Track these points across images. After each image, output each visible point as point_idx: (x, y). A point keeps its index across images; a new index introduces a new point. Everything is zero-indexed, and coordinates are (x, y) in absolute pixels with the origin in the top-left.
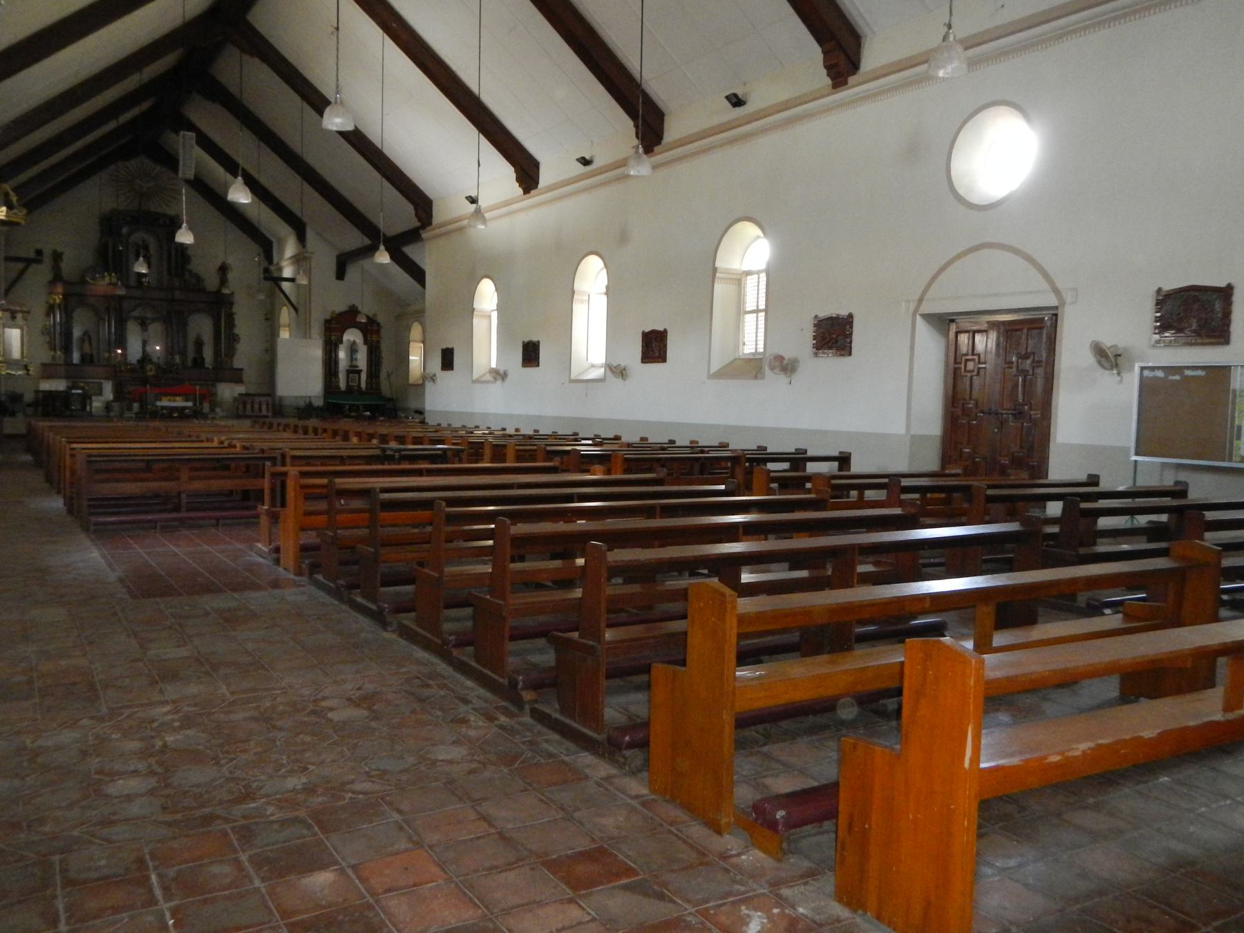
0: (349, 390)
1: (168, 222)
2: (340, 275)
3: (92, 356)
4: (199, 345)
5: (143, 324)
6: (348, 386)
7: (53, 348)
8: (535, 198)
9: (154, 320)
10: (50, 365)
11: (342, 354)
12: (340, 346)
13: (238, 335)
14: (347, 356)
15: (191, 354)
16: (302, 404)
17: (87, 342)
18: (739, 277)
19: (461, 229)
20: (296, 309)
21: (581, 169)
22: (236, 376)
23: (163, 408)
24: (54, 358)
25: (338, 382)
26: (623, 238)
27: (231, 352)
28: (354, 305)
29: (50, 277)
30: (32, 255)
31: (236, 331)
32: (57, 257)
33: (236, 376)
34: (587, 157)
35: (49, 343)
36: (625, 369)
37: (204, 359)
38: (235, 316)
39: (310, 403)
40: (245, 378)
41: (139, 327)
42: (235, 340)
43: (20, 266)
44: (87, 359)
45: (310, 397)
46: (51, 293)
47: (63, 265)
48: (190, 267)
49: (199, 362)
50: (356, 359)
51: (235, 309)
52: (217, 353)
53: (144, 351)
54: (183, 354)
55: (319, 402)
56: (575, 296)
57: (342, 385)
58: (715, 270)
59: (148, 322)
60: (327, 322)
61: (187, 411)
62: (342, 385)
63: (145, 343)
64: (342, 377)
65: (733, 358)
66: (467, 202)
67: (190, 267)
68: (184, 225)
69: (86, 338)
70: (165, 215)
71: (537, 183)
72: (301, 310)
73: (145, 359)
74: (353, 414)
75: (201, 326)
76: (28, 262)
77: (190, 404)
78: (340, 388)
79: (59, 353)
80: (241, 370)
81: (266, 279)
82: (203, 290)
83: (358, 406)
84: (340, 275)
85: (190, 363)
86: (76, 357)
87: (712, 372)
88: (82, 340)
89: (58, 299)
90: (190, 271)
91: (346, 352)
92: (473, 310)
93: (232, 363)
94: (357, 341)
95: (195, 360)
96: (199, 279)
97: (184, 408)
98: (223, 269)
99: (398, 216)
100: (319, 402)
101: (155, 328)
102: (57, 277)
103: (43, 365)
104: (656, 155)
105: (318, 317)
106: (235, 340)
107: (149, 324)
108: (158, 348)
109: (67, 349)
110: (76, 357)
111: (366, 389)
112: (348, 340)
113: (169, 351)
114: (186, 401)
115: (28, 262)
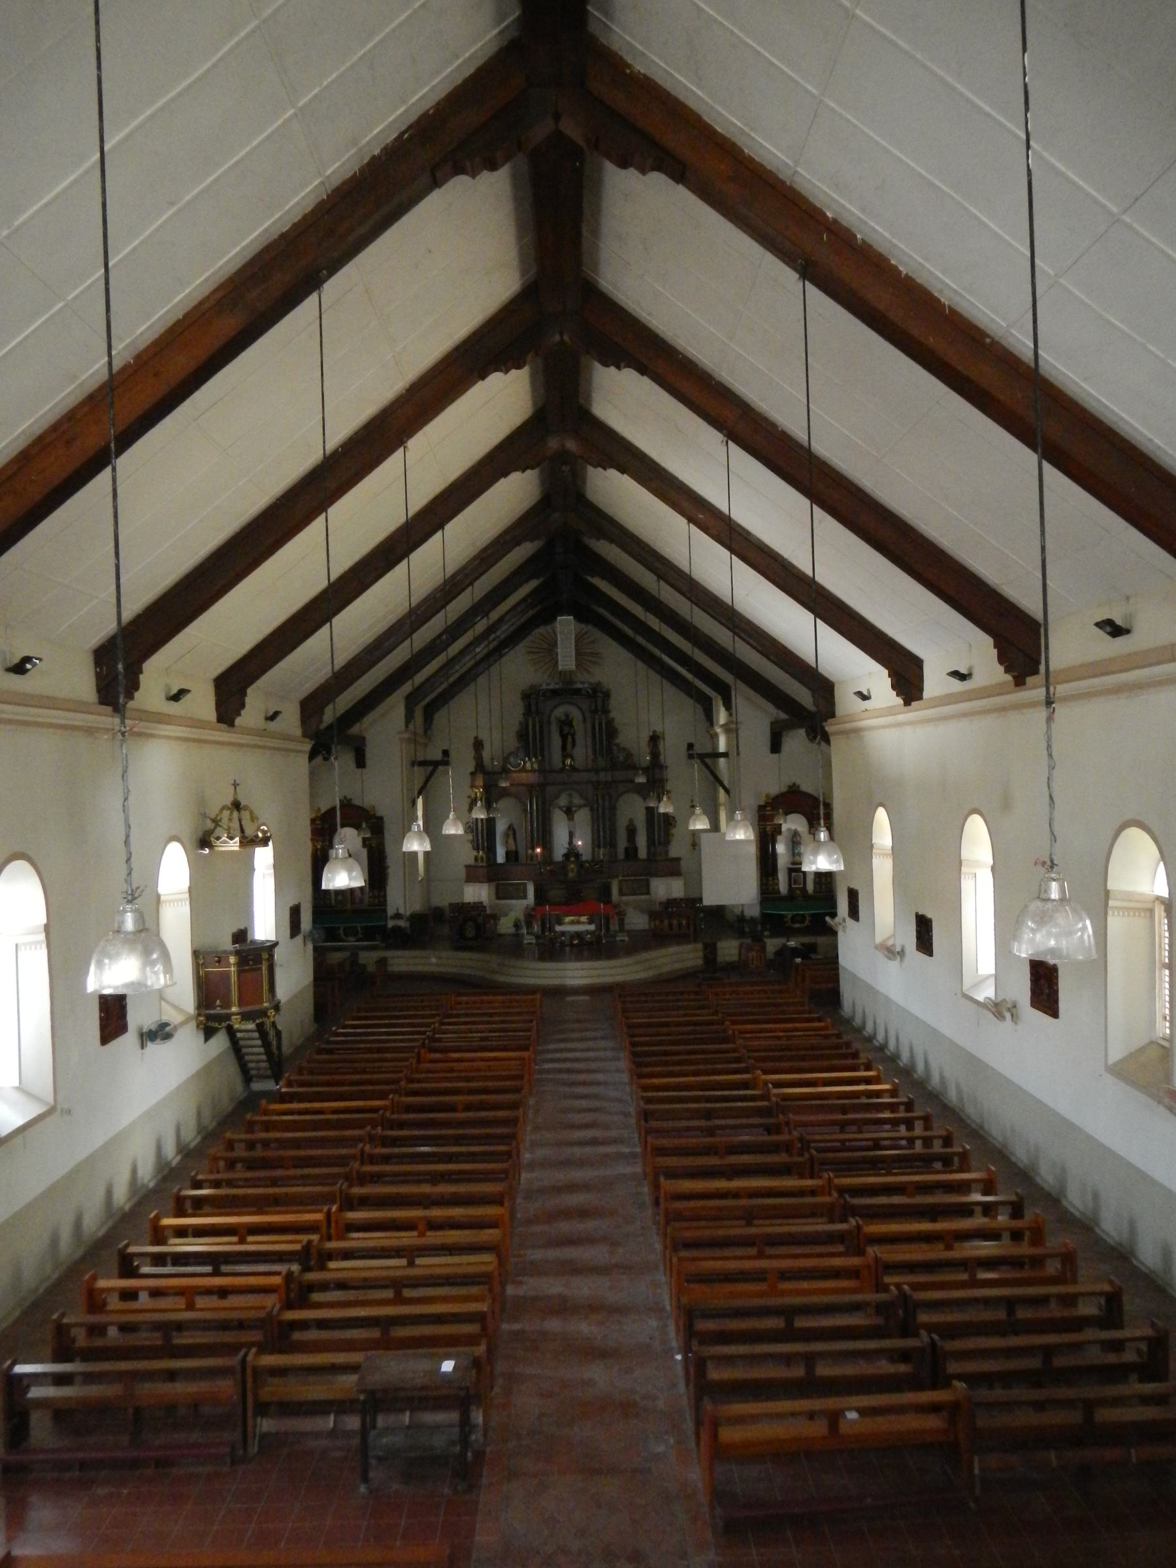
0: (791, 896)
2: (776, 747)
3: (516, 853)
4: (632, 832)
5: (569, 812)
6: (790, 889)
7: (477, 848)
8: (917, 712)
9: (580, 807)
11: (781, 848)
12: (779, 838)
14: (787, 849)
15: (622, 843)
16: (738, 911)
17: (511, 837)
18: (1149, 906)
19: (857, 731)
21: (957, 686)
22: (673, 869)
23: (563, 933)
24: (476, 859)
25: (777, 884)
26: (1006, 804)
27: (667, 842)
28: (794, 784)
29: (473, 769)
30: (438, 756)
32: (478, 745)
33: (673, 869)
34: (963, 671)
35: (472, 842)
36: (1015, 1007)
39: (742, 912)
41: (565, 815)
42: (671, 824)
44: (512, 856)
45: (742, 905)
46: (472, 786)
47: (486, 754)
48: (617, 741)
49: (631, 852)
50: (799, 854)
52: (651, 843)
54: (613, 845)
55: (754, 912)
56: (963, 869)
57: (783, 887)
58: (1107, 893)
59: (574, 809)
60: (761, 808)
62: (783, 887)
63: (571, 835)
64: (782, 877)
65: (1147, 1041)
66: (859, 700)
67: (617, 741)
68: (451, 815)
69: (511, 833)
71: (920, 689)
72: (732, 792)
73: (572, 853)
74: (797, 925)
75: (632, 809)
76: (435, 764)
77: (592, 927)
78: (779, 892)
79: (481, 853)
80: (678, 859)
81: (691, 757)
83: (803, 916)
84: (776, 747)
85: (621, 854)
86: (501, 858)
87: (1111, 1061)
88: (506, 835)
89: (479, 791)
90: (618, 745)
91: (786, 845)
92: (872, 846)
93: (667, 852)
94: (800, 829)
95: (626, 850)
96: (629, 755)
97: (588, 932)
98: (655, 739)
99: (803, 696)
100: (754, 912)
101: (583, 816)
102: (480, 767)
103: (467, 867)
104: (1026, 690)
105: (751, 799)
106: (671, 824)
108: (580, 843)
109: (491, 850)
110: (501, 858)
111: (814, 891)
112: (789, 830)
113: (596, 844)
115: (435, 764)
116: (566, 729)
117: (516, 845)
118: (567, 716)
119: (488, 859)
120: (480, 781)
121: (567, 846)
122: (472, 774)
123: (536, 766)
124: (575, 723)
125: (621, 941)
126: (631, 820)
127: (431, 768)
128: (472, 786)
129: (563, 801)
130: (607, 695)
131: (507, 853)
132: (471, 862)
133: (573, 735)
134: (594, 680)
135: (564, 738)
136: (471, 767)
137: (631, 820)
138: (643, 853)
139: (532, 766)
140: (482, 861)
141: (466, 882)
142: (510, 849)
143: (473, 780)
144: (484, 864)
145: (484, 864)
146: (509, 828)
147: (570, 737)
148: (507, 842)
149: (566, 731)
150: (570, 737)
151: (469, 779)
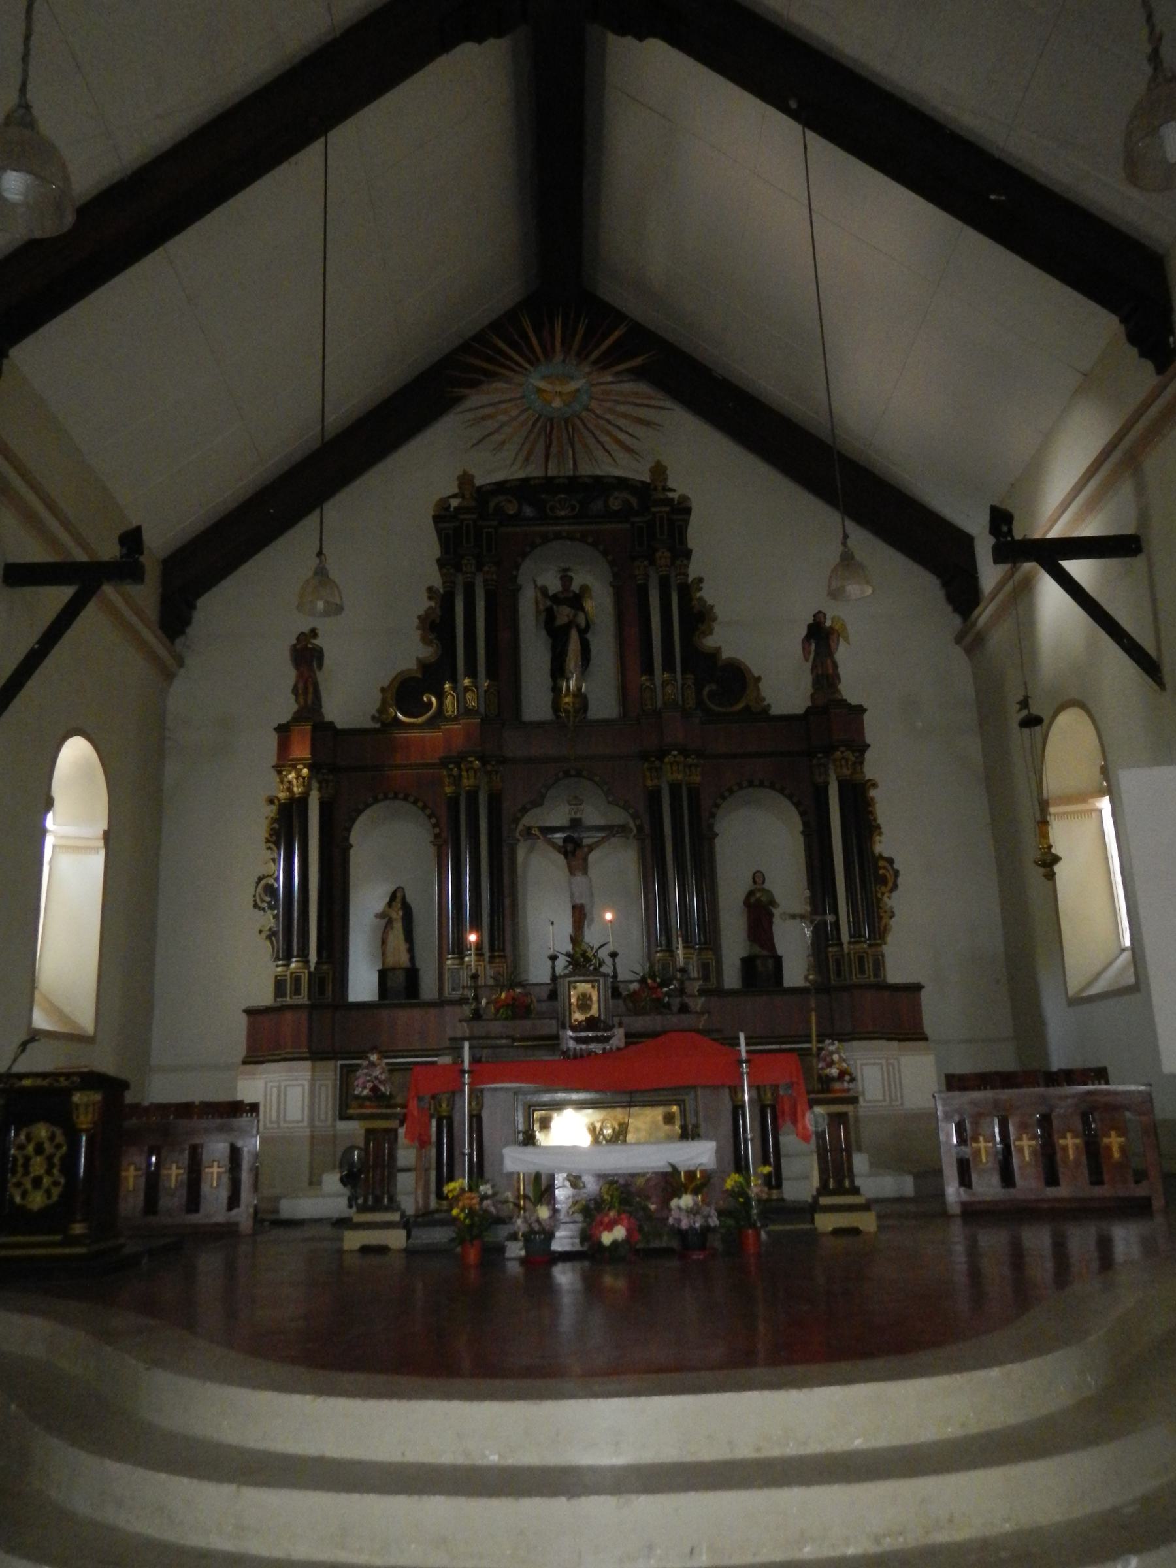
1: (634, 501)
3: (412, 974)
10: (266, 1011)
13: (891, 861)
17: (398, 926)
20: (1149, 666)
24: (279, 986)
29: (285, 718)
31: (882, 846)
37: (778, 960)
38: (873, 793)
40: (929, 1025)
41: (562, 857)
42: (883, 881)
43: (58, 596)
48: (710, 642)
51: (871, 770)
52: (824, 938)
53: (576, 939)
61: (686, 1201)
63: (580, 915)
67: (710, 642)
69: (397, 915)
70: (622, 483)
80: (917, 988)
82: (761, 715)
85: (732, 978)
95: (748, 963)
106: (883, 881)
107: (591, 848)
108: (609, 916)
114: (688, 1134)
116: (564, 614)
117: (411, 950)
118: (566, 579)
119: (318, 982)
120: (301, 750)
121: (569, 947)
122: (283, 730)
123: (471, 700)
124: (589, 605)
125: (838, 1232)
126: (758, 878)
127: (62, 594)
128: (279, 769)
129: (557, 815)
130: (682, 509)
131: (383, 974)
132: (265, 997)
133: (583, 632)
134: (640, 473)
135: (557, 636)
136: (285, 708)
137: (758, 878)
138: (796, 972)
139: (462, 701)
140: (297, 991)
141: (245, 1063)
142: (391, 961)
143: (284, 747)
144: (303, 999)
145: (303, 999)
146: (393, 897)
147: (574, 636)
148: (384, 942)
149: (561, 620)
150: (574, 636)
151: (272, 740)
